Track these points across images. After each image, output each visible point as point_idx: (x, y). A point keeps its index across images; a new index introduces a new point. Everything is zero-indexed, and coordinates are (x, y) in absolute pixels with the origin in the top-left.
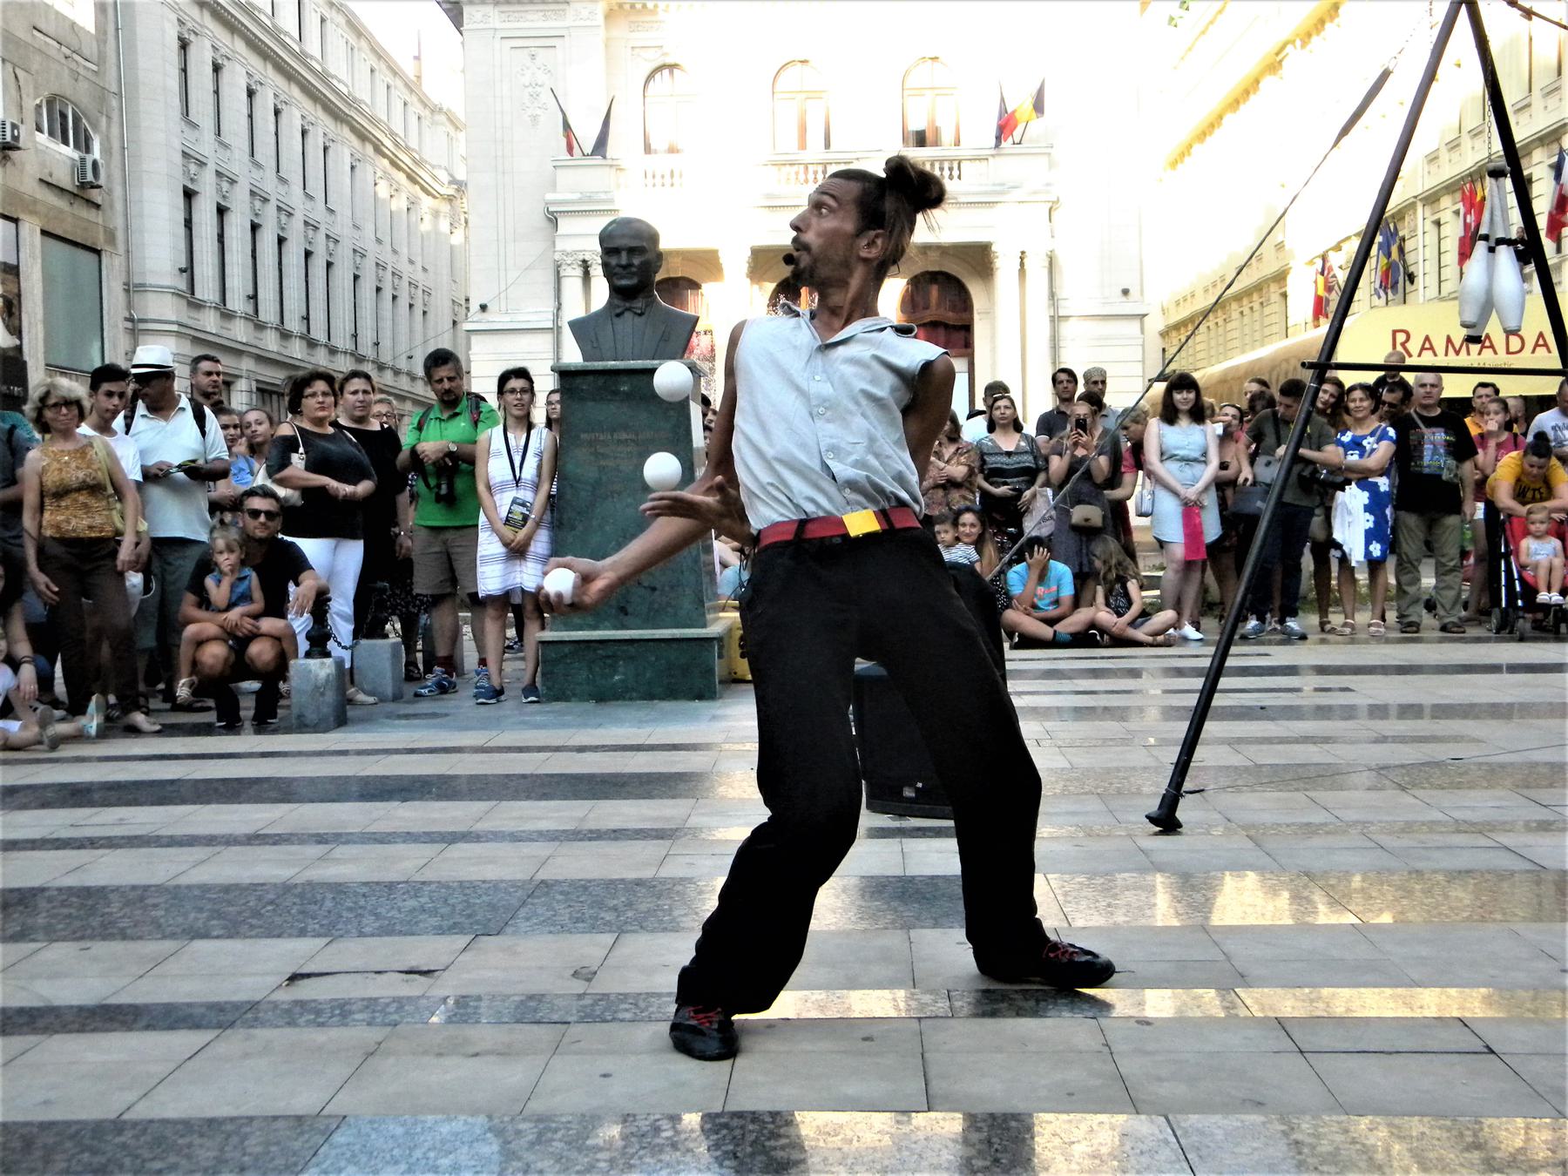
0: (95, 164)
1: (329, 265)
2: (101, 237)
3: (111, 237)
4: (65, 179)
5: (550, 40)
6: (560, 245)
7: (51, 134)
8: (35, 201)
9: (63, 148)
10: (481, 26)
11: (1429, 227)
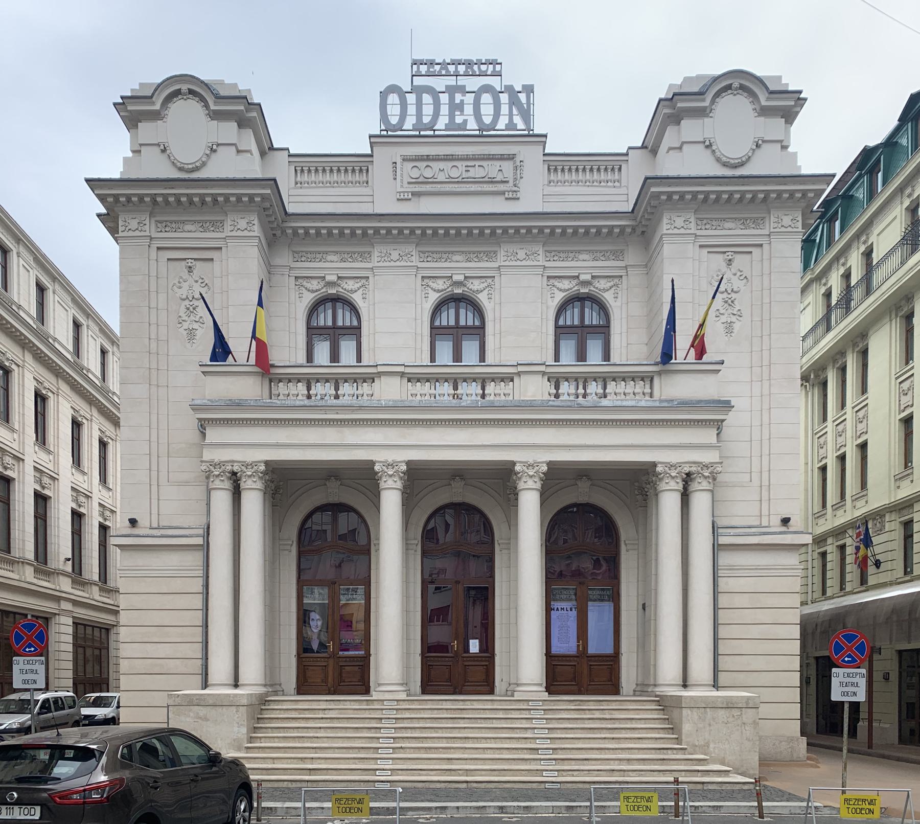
5: (207, 254)
10: (137, 233)
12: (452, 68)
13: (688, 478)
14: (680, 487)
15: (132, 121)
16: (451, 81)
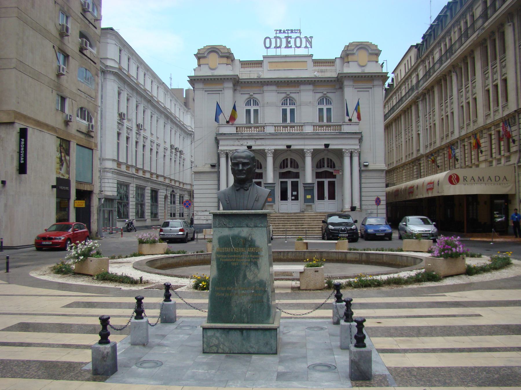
0: (92, 126)
1: (157, 152)
2: (93, 145)
3: (96, 146)
4: (84, 130)
6: (220, 148)
7: (81, 118)
8: (75, 136)
9: (84, 121)
11: (462, 146)
12: (287, 32)
13: (351, 153)
14: (349, 155)
15: (200, 56)
16: (286, 35)
